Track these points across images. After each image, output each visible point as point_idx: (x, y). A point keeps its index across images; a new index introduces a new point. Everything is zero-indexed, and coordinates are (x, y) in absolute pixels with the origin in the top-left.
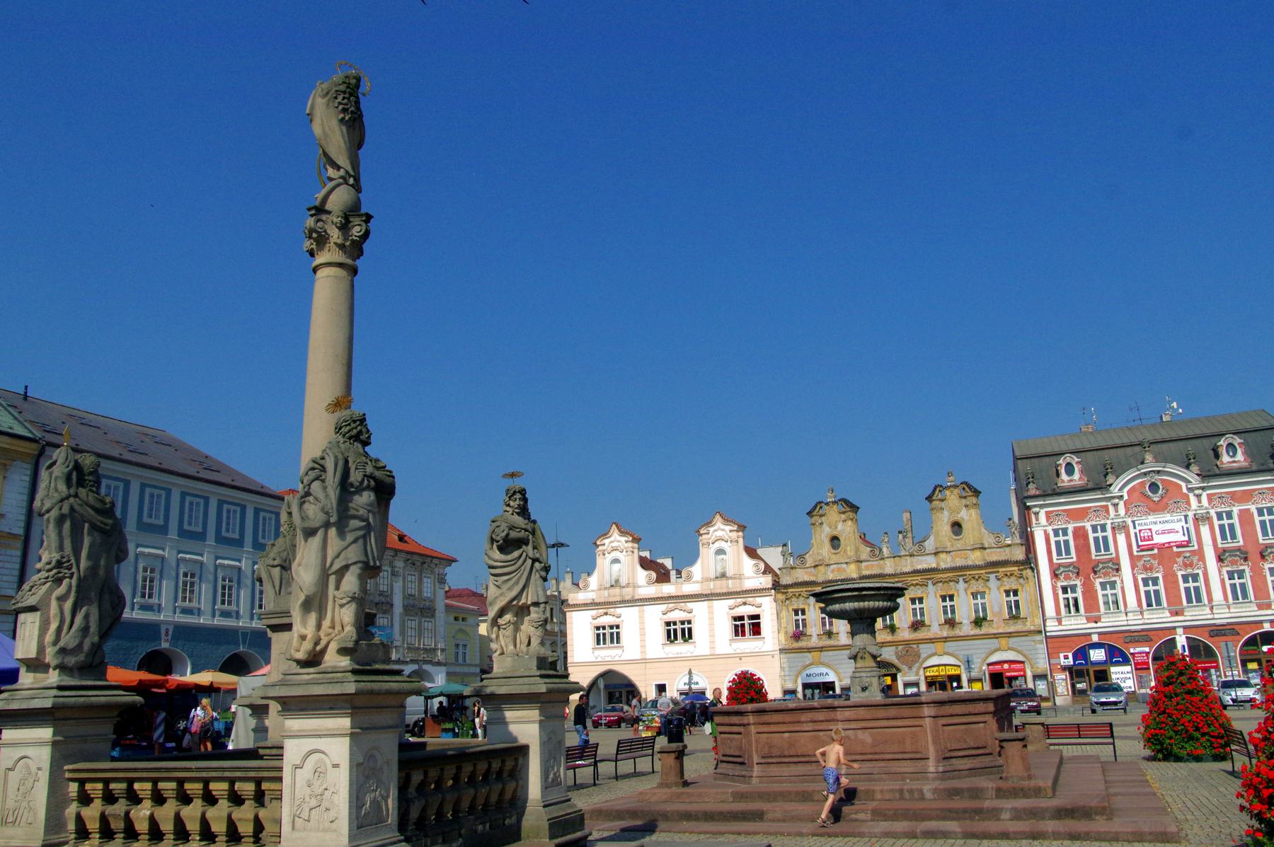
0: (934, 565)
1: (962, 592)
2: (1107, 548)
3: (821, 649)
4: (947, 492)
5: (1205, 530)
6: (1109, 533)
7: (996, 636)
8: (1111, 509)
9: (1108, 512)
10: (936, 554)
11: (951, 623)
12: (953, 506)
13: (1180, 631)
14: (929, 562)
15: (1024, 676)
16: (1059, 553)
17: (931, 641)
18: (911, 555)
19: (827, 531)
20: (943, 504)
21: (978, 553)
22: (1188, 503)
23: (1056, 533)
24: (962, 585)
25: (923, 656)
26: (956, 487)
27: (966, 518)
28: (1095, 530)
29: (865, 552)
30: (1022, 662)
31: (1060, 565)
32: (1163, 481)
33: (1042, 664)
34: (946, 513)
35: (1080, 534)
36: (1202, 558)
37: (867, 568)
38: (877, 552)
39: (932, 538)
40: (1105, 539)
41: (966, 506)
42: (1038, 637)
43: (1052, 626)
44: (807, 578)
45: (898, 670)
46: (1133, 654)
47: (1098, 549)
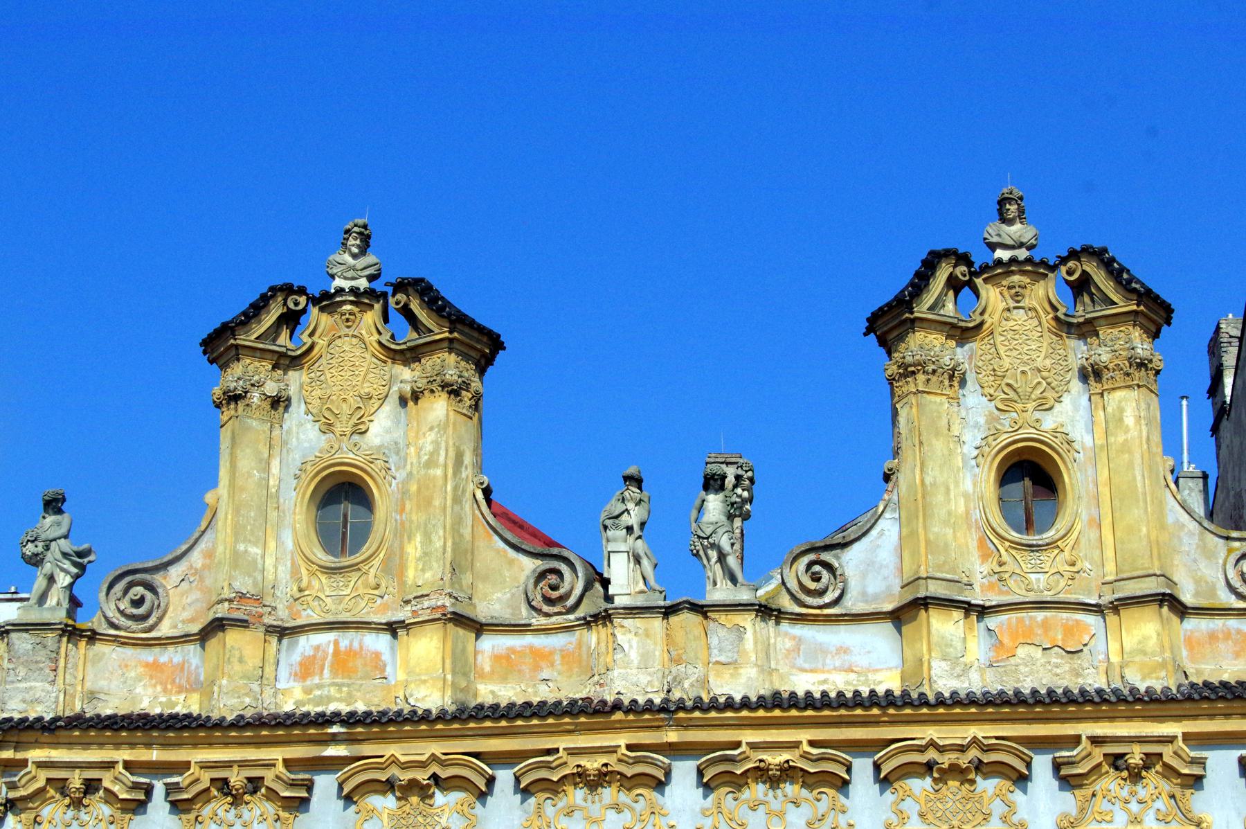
0: (889, 681)
4: (992, 295)
10: (902, 616)
12: (1016, 367)
14: (865, 660)
18: (766, 611)
19: (304, 441)
20: (961, 355)
21: (1145, 628)
26: (1039, 268)
27: (1081, 435)
29: (504, 580)
34: (975, 403)
37: (506, 665)
38: (574, 583)
39: (888, 529)
41: (1091, 374)
44: (150, 699)
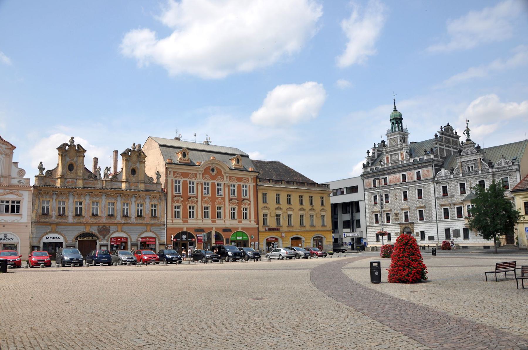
1: (133, 203)
2: (193, 192)
3: (58, 224)
5: (227, 189)
6: (195, 185)
7: (146, 225)
8: (198, 175)
9: (196, 176)
11: (126, 216)
13: (214, 229)
15: (155, 244)
16: (176, 191)
17: (117, 224)
22: (223, 179)
23: (176, 182)
24: (133, 199)
25: (111, 232)
28: (190, 183)
30: (155, 238)
31: (176, 196)
32: (217, 168)
33: (163, 239)
35: (185, 183)
36: (224, 201)
40: (193, 187)
42: (163, 227)
43: (169, 221)
45: (98, 238)
46: (197, 237)
47: (190, 192)
